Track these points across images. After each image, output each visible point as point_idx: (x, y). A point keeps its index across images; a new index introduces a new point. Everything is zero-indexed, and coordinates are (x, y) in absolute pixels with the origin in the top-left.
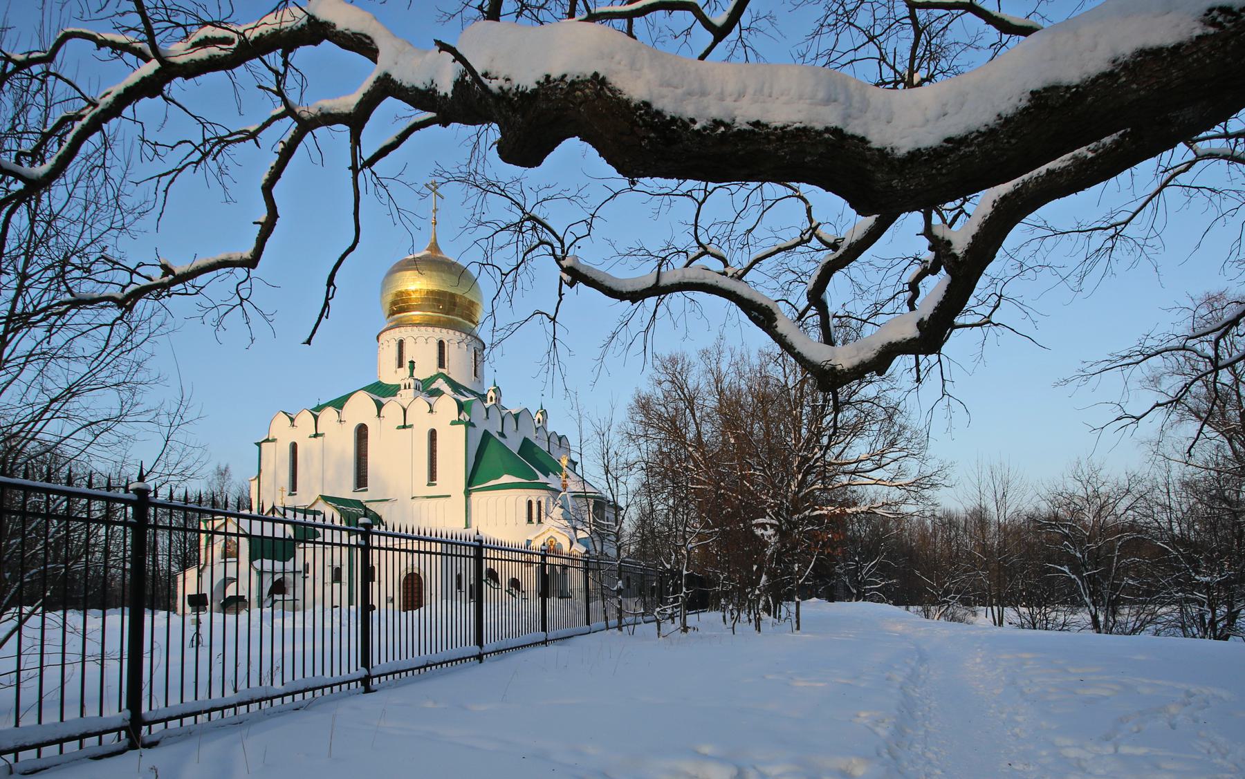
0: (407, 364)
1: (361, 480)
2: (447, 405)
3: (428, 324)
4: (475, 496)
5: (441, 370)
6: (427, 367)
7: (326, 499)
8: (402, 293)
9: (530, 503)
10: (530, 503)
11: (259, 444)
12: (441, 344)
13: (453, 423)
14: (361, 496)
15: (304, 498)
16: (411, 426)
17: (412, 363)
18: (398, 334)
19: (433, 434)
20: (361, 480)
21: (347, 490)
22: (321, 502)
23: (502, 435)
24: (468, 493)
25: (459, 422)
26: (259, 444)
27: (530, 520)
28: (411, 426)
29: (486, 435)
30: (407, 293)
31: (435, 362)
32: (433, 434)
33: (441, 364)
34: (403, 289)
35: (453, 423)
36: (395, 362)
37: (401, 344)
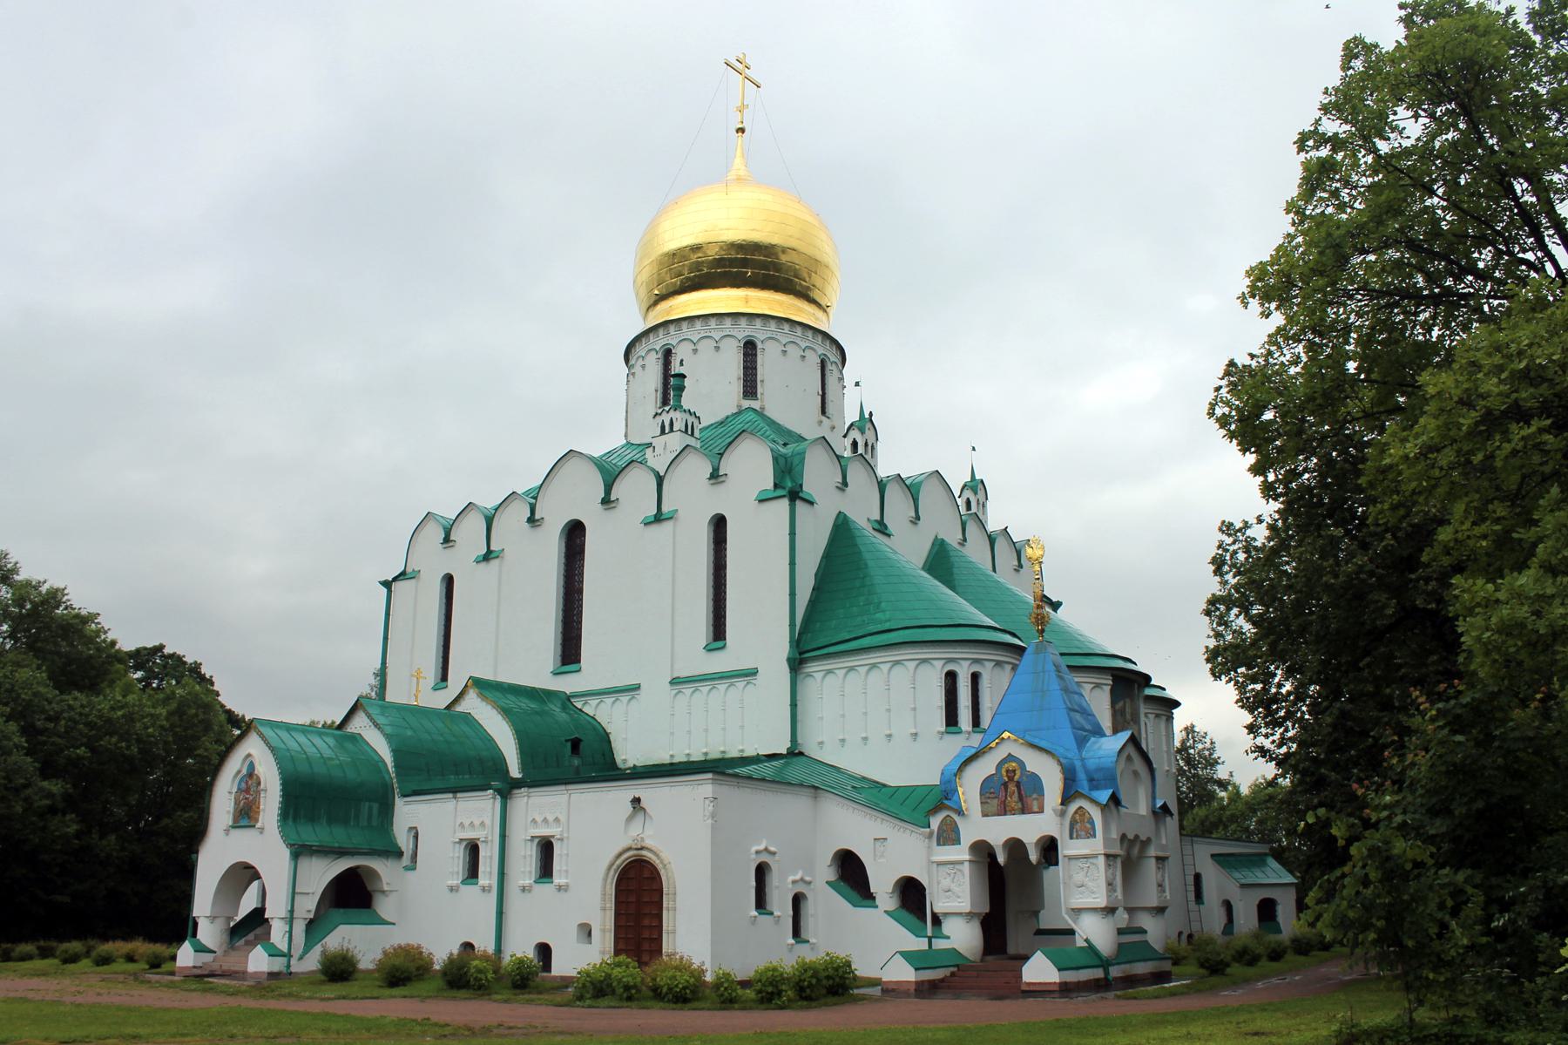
1: (570, 652)
2: (752, 465)
5: (746, 403)
9: (951, 677)
10: (951, 677)
11: (387, 584)
12: (750, 348)
14: (568, 684)
18: (658, 341)
20: (570, 652)
22: (472, 695)
23: (881, 527)
24: (797, 662)
26: (387, 584)
27: (952, 719)
29: (842, 529)
31: (737, 387)
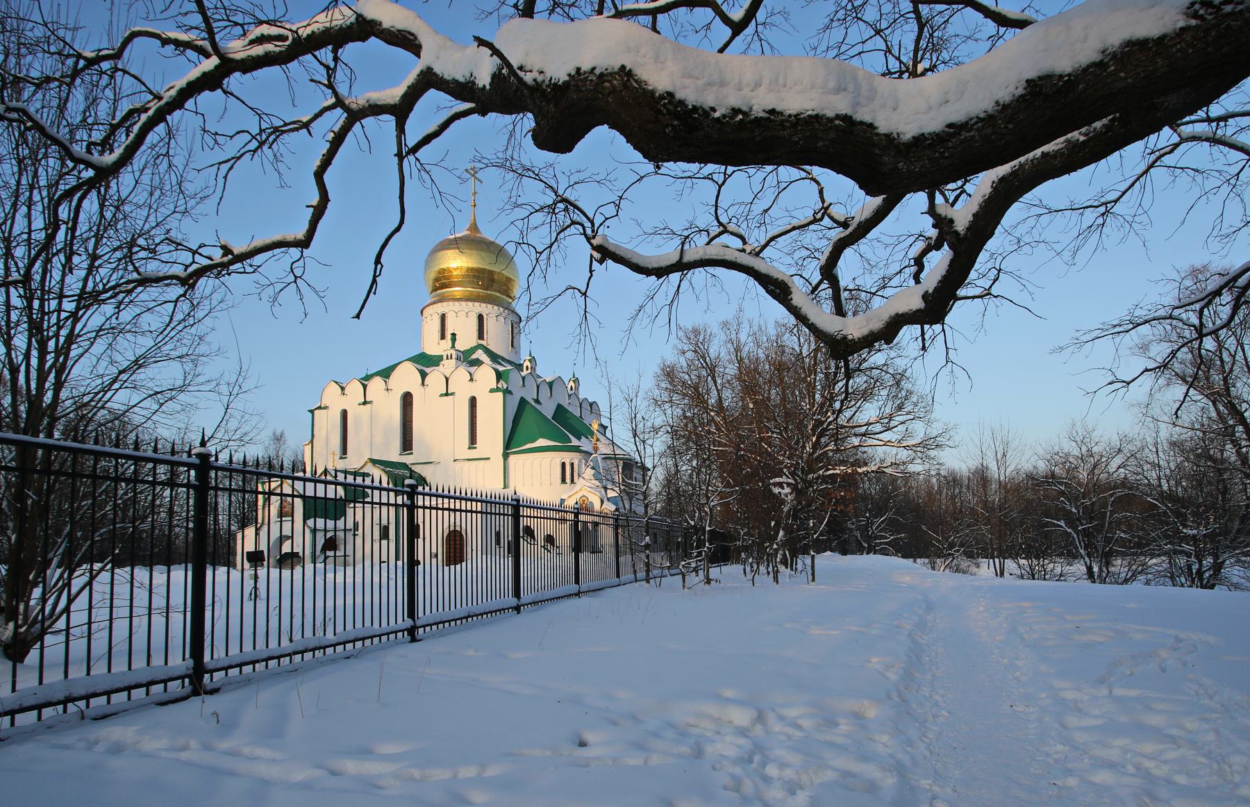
0: (449, 336)
1: (407, 445)
2: (486, 374)
3: (468, 300)
4: (513, 459)
5: (480, 342)
6: (467, 339)
7: (374, 462)
8: (444, 270)
9: (563, 465)
10: (563, 465)
11: (312, 412)
12: (480, 318)
13: (492, 391)
14: (407, 459)
15: (354, 461)
16: (453, 394)
17: (454, 335)
19: (473, 401)
20: (407, 445)
21: (394, 455)
22: (370, 465)
23: (537, 401)
24: (506, 456)
25: (497, 390)
26: (312, 412)
27: (563, 480)
28: (453, 394)
29: (523, 402)
30: (449, 270)
31: (475, 334)
32: (473, 401)
33: (481, 336)
34: (445, 266)
35: (492, 391)
36: (437, 334)
37: (443, 318)
